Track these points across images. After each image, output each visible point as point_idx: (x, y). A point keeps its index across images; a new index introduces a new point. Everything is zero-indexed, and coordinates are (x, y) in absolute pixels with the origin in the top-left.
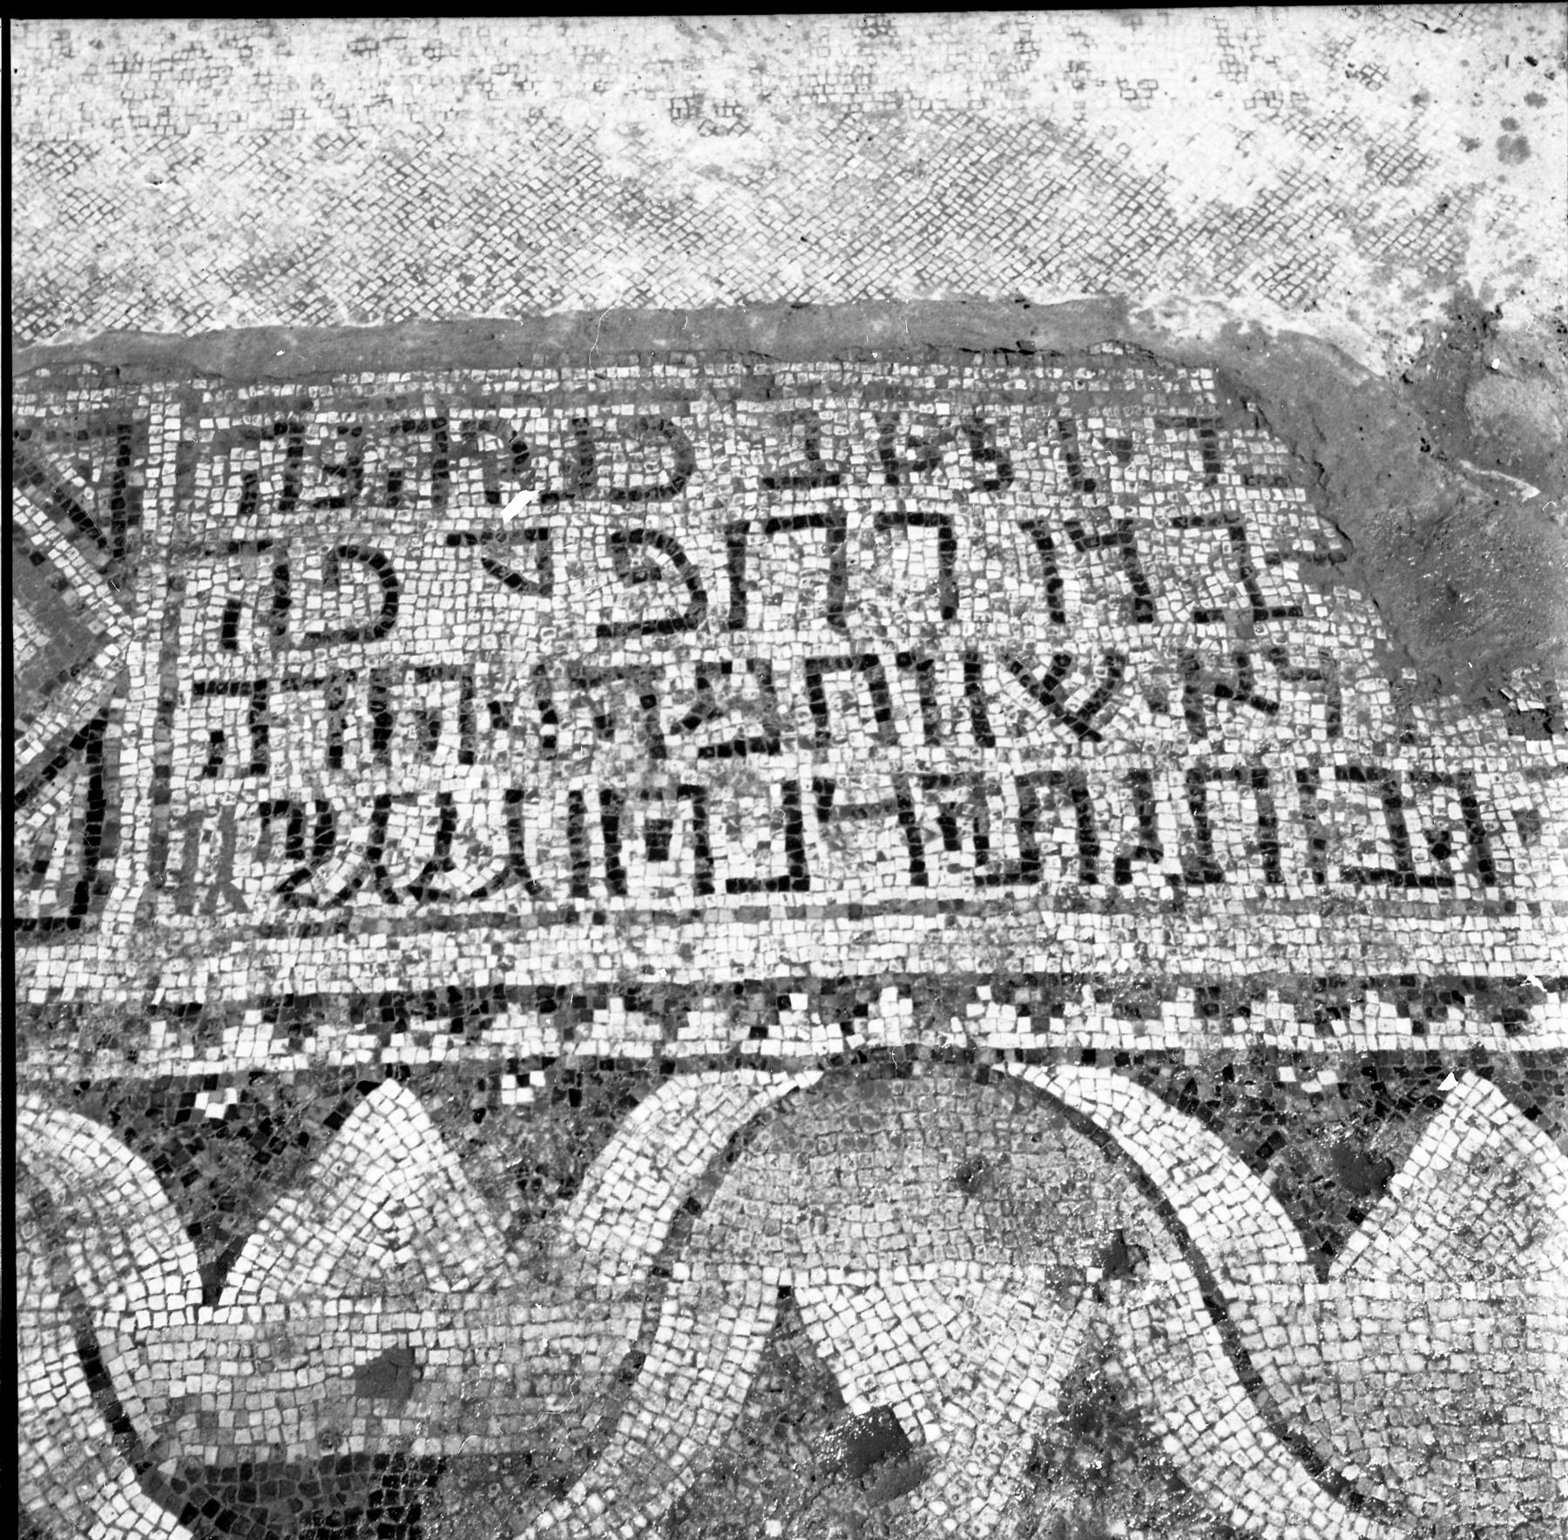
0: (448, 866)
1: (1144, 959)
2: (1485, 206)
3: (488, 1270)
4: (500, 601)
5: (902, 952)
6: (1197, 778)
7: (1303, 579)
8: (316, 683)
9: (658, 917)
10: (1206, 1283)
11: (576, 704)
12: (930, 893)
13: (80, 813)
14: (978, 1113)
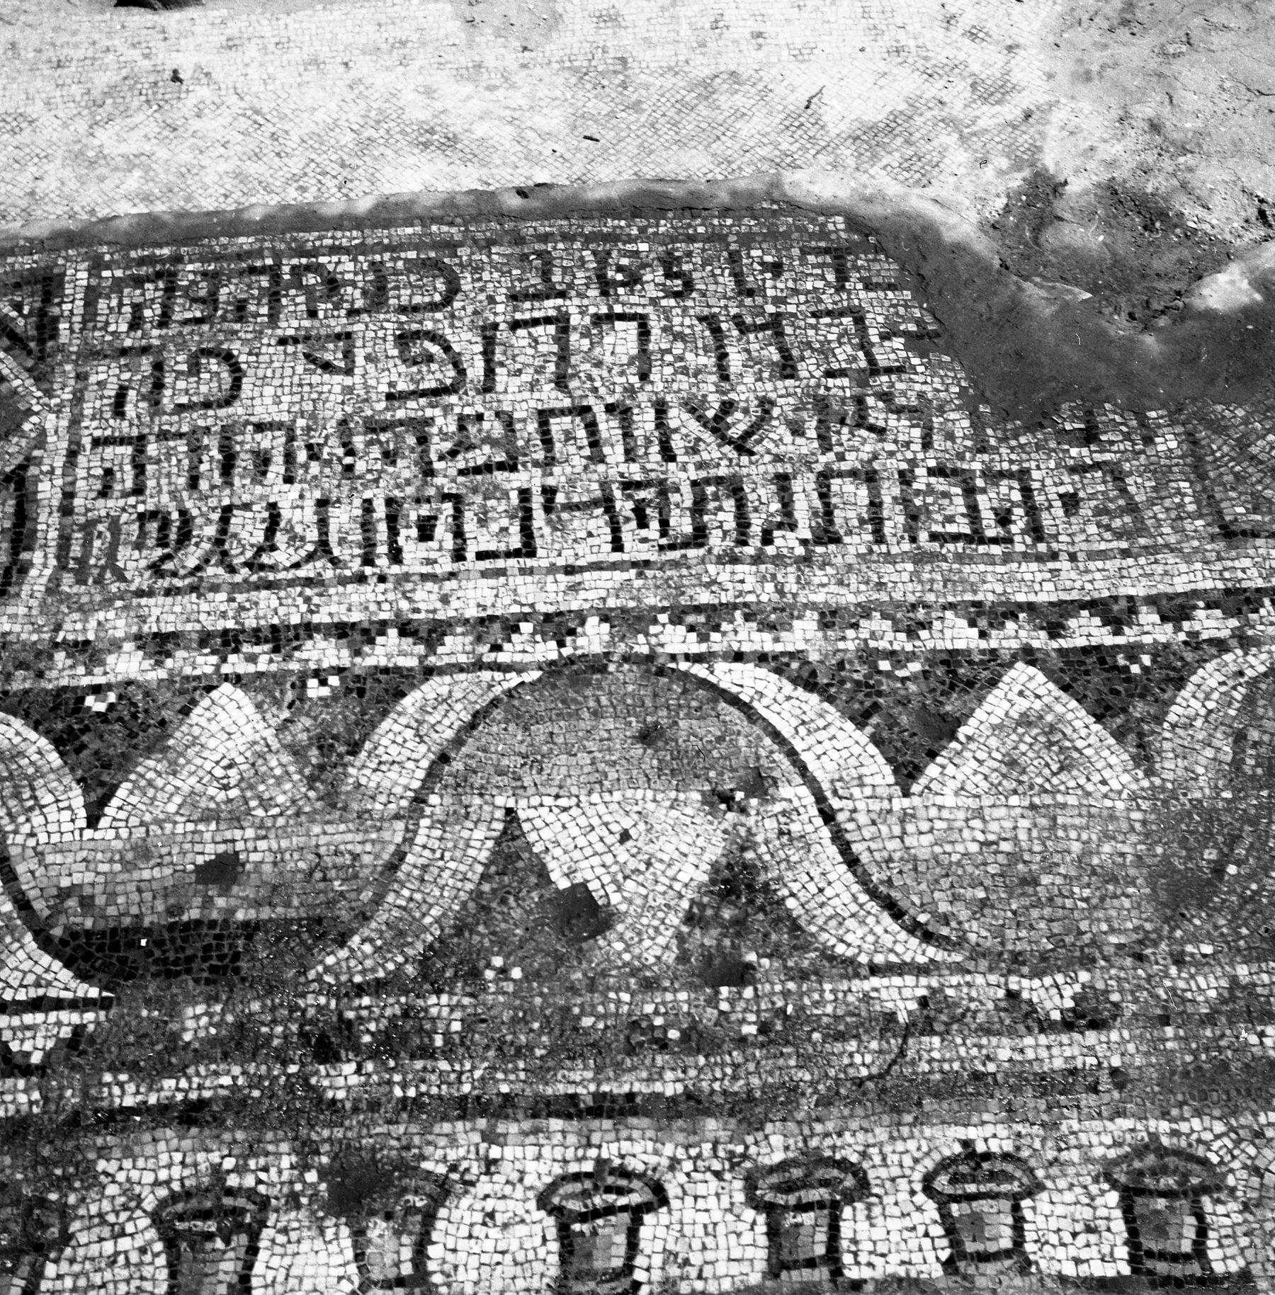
0: (273, 548)
1: (781, 592)
2: (1058, 116)
3: (294, 802)
4: (315, 379)
5: (603, 594)
6: (825, 477)
7: (907, 348)
8: (180, 435)
9: (424, 577)
10: (820, 799)
11: (369, 444)
12: (625, 557)
14: (655, 695)
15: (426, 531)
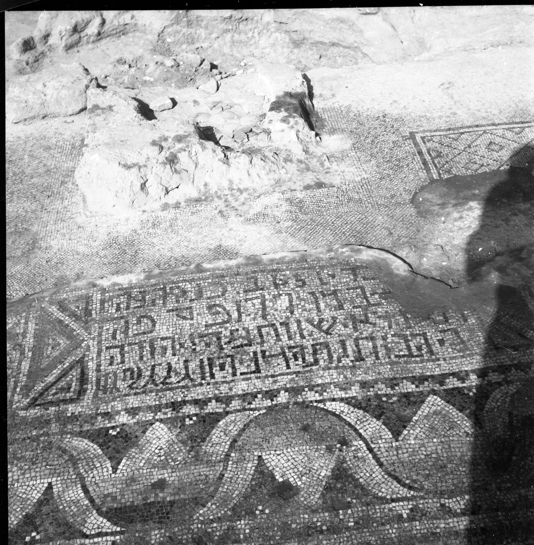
0: (170, 377)
3: (184, 459)
4: (181, 322)
5: (285, 383)
6: (357, 340)
9: (223, 382)
10: (367, 445)
12: (292, 370)
13: (78, 377)
15: (222, 367)
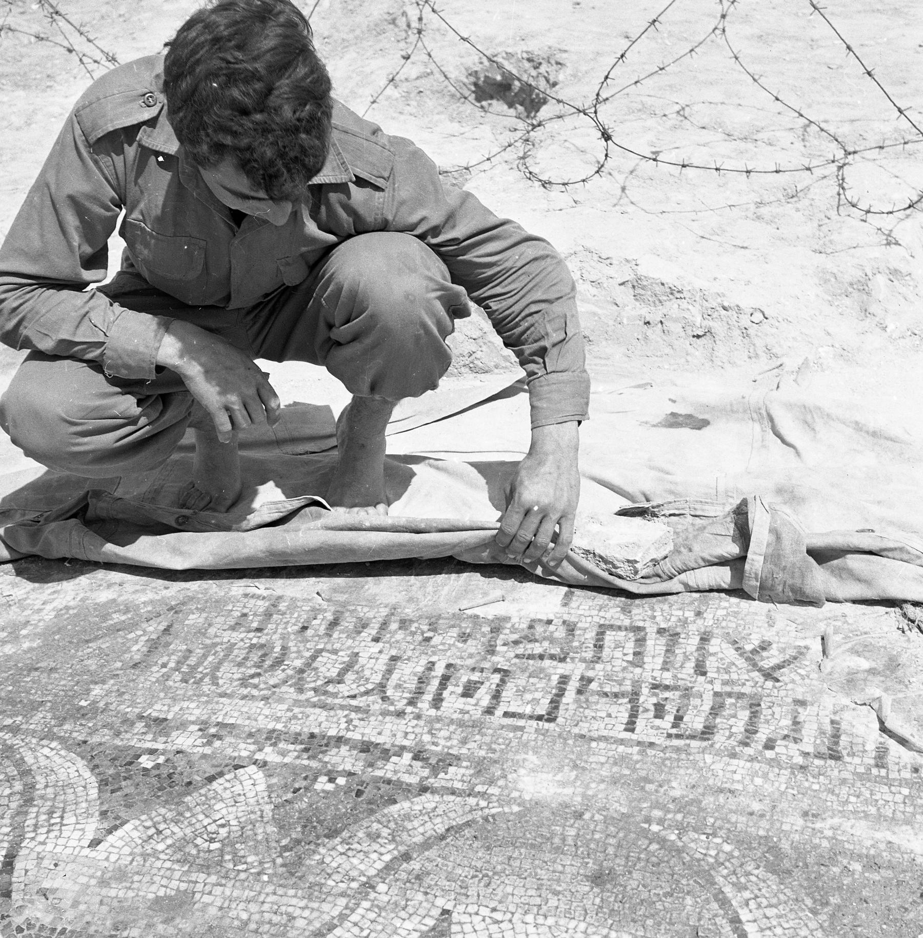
12: (634, 737)
15: (469, 691)
